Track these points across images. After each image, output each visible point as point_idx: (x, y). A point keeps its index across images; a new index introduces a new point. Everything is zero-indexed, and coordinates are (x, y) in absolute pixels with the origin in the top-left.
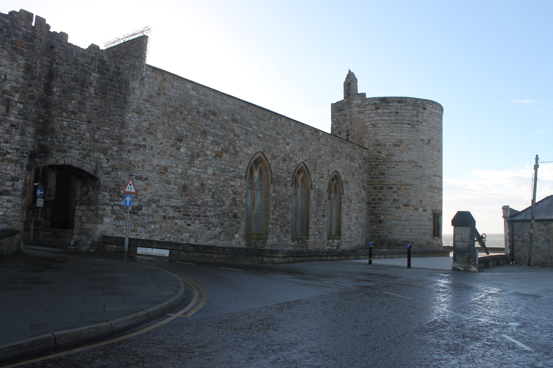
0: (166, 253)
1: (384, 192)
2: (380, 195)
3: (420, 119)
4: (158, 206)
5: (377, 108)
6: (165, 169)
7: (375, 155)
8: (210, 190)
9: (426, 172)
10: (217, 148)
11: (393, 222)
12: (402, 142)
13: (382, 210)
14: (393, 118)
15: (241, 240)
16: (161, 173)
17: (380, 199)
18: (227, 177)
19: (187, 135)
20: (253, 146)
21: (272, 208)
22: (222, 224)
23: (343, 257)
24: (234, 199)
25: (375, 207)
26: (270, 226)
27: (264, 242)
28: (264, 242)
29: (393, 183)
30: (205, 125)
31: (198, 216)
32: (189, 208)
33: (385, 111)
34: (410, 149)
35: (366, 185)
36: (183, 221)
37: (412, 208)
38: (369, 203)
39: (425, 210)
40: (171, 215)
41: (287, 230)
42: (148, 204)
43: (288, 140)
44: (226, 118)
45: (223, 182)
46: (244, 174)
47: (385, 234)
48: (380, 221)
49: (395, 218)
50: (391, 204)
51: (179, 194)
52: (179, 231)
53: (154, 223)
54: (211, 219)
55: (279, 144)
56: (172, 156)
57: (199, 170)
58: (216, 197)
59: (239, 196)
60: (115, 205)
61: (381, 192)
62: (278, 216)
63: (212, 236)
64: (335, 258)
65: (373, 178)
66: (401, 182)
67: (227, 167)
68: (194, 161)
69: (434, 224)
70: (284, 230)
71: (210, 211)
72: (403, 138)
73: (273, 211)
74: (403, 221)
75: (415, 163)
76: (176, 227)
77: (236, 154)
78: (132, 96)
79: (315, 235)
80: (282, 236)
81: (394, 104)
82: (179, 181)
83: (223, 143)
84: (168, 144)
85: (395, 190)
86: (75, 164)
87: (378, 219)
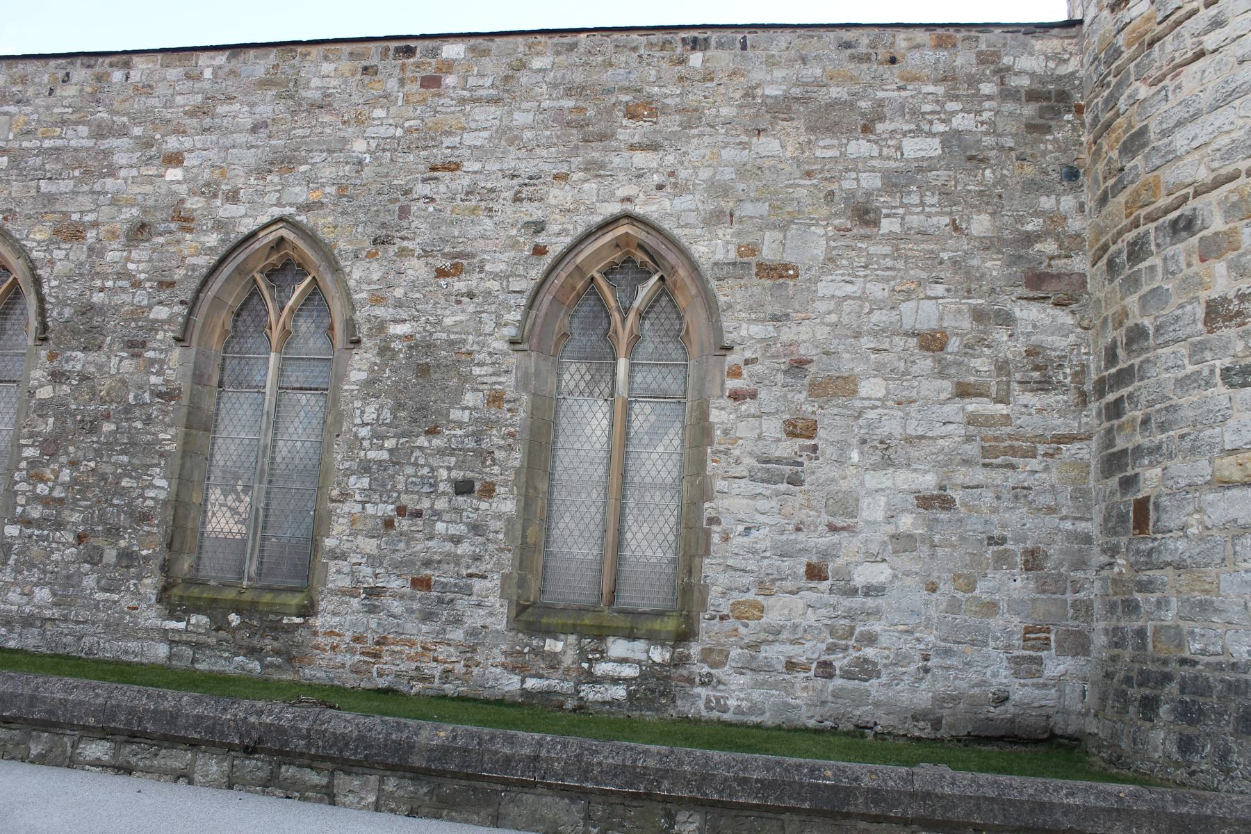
1: (1152, 268)
2: (1132, 301)
13: (1145, 422)
17: (1137, 335)
21: (30, 452)
25: (1115, 410)
26: (12, 530)
29: (1203, 175)
41: (127, 557)
43: (173, 143)
47: (1170, 616)
49: (1229, 468)
50: (1197, 351)
55: (112, 174)
62: (67, 487)
70: (110, 555)
73: (33, 463)
79: (374, 592)
80: (90, 582)
85: (1218, 224)
87: (1130, 498)
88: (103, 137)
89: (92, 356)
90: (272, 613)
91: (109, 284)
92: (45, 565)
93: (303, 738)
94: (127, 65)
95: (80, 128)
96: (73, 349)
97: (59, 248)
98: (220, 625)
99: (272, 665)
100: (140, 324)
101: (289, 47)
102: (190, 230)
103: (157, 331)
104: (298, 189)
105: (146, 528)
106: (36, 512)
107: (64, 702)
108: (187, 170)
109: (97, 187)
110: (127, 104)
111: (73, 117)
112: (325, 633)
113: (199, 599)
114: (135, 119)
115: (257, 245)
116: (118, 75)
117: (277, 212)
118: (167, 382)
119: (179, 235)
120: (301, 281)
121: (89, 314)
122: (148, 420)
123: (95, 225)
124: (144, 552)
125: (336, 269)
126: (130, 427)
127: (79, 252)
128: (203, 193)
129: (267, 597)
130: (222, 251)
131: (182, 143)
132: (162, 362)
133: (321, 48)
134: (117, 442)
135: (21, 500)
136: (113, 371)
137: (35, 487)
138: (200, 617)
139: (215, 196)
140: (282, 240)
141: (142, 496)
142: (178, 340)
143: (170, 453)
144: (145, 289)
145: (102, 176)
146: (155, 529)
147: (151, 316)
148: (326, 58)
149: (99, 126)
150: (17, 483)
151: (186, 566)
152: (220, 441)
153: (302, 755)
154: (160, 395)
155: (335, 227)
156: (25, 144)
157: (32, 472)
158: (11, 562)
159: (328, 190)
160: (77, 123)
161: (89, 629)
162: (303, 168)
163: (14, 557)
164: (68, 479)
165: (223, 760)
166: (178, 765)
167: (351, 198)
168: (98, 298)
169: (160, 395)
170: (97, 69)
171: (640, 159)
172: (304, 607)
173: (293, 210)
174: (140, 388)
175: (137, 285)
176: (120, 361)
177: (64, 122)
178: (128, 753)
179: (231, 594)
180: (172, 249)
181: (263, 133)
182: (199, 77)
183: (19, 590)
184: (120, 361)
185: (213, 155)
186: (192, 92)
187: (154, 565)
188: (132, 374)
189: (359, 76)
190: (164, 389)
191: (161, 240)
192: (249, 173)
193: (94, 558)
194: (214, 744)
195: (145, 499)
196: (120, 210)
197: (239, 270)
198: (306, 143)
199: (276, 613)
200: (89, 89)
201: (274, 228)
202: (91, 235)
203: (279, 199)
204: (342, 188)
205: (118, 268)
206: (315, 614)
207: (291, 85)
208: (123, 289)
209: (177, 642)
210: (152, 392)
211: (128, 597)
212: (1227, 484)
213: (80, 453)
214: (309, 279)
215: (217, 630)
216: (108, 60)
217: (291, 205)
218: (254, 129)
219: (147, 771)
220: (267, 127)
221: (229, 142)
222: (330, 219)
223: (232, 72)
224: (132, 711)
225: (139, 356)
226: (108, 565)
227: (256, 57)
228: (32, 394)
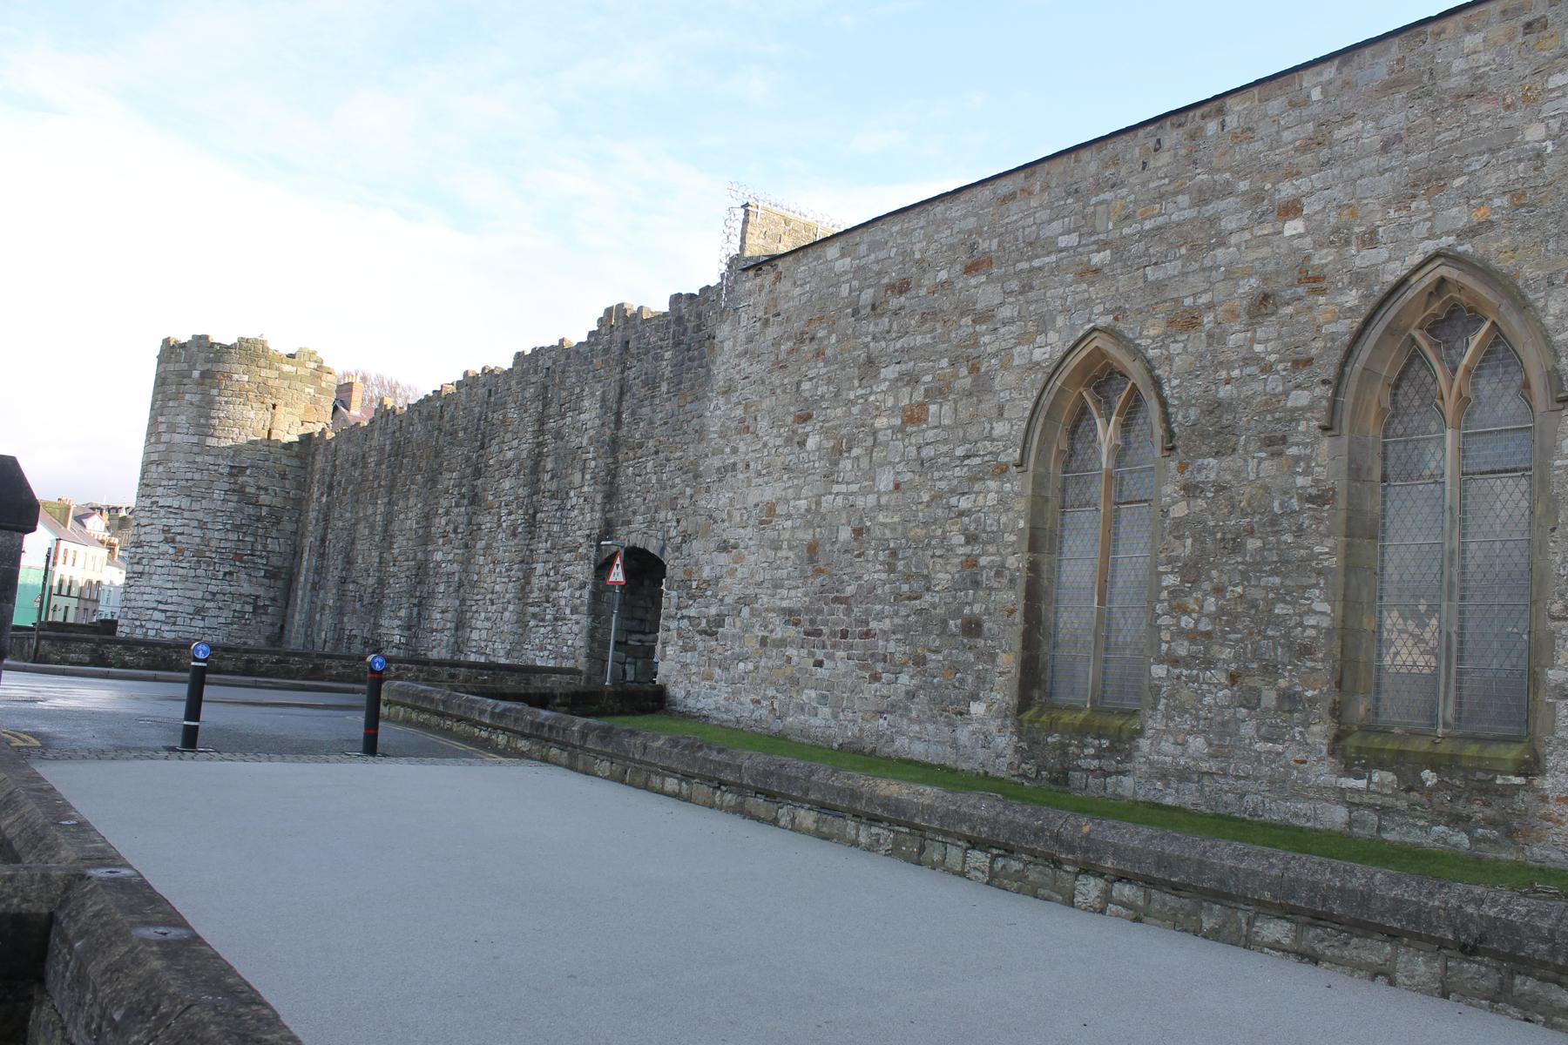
4: (753, 613)
6: (771, 509)
8: (883, 544)
15: (993, 726)
16: (761, 523)
18: (942, 485)
20: (1060, 321)
21: (1170, 580)
22: (920, 661)
23: (554, 751)
24: (971, 562)
26: (1159, 671)
27: (1112, 750)
28: (1112, 750)
31: (844, 634)
32: (820, 612)
36: (804, 652)
40: (778, 634)
41: (1289, 700)
43: (1287, 190)
44: (943, 275)
45: (928, 505)
46: (1017, 455)
51: (797, 574)
52: (794, 681)
53: (745, 659)
54: (881, 643)
58: (900, 565)
59: (991, 549)
60: (683, 617)
63: (884, 705)
64: (523, 745)
67: (943, 449)
68: (837, 464)
70: (1269, 698)
71: (880, 617)
73: (1174, 592)
76: (788, 670)
77: (982, 385)
80: (1248, 729)
82: (800, 534)
83: (926, 372)
86: (640, 545)
88: (1206, 202)
89: (1227, 461)
90: (1480, 769)
91: (1236, 373)
92: (1197, 710)
93: (1544, 940)
94: (1221, 111)
95: (1180, 198)
96: (1204, 456)
97: (1176, 341)
98: (1411, 785)
99: (1485, 839)
100: (1277, 415)
101: (1414, 31)
102: (1323, 292)
103: (1298, 421)
104: (1455, 210)
105: (1309, 664)
106: (1182, 649)
107: (1234, 871)
108: (1308, 218)
109: (1208, 262)
110: (1228, 157)
111: (1171, 188)
112: (1559, 799)
113: (1383, 750)
114: (1239, 174)
115: (1410, 294)
116: (1212, 127)
117: (1430, 246)
118: (1317, 482)
119: (1309, 300)
120: (1476, 329)
121: (1217, 413)
122: (1300, 532)
123: (1211, 306)
124: (1309, 694)
125: (1522, 305)
126: (1278, 542)
127: (1197, 341)
128: (1332, 242)
129: (1472, 750)
130: (1365, 310)
131: (1298, 188)
132: (1308, 459)
133: (1458, 18)
134: (1265, 561)
135: (1165, 636)
136: (1252, 476)
137: (1179, 620)
138: (1384, 774)
139: (1348, 243)
140: (1442, 281)
141: (1301, 624)
142: (1325, 429)
143: (1330, 570)
144: (1277, 372)
145: (1212, 248)
146: (1321, 665)
147: (1289, 404)
148: (1469, 29)
149: (1200, 191)
150: (1159, 616)
151: (1362, 710)
152: (1390, 550)
153: (1543, 964)
154: (1311, 499)
155: (1514, 250)
156: (1126, 231)
157: (1174, 603)
158: (1161, 707)
159: (1497, 202)
160: (1176, 194)
161: (1252, 786)
162: (1458, 182)
163: (1163, 701)
164: (1213, 609)
165: (1435, 960)
166: (1374, 959)
167: (1532, 207)
168: (1225, 392)
169: (1311, 499)
170: (1189, 126)
172: (1525, 762)
173: (1452, 239)
174: (1286, 493)
175: (1268, 369)
176: (1259, 463)
177: (1162, 196)
178: (1313, 938)
179: (1422, 745)
180: (1303, 319)
181: (1397, 150)
182: (1307, 101)
183: (1171, 739)
184: (1259, 463)
185: (1337, 192)
186: (1301, 122)
187: (1322, 709)
188: (1274, 477)
189: (1520, 39)
190: (1314, 491)
191: (1289, 310)
192: (1387, 204)
193: (1251, 701)
194: (1419, 937)
195: (1305, 628)
196: (1237, 285)
197: (1391, 330)
198: (1457, 148)
199: (1487, 771)
200: (1183, 152)
201: (1430, 267)
202: (1208, 319)
203: (1430, 229)
204: (1517, 197)
205: (1243, 352)
206: (1542, 773)
207: (1425, 78)
208: (1252, 377)
209: (1357, 805)
210: (1300, 497)
211: (1294, 747)
213: (1225, 578)
214: (1487, 325)
215: (1409, 790)
216: (1198, 112)
217: (1448, 234)
218: (1386, 147)
219: (1337, 962)
220: (1401, 140)
221: (1355, 172)
222: (1505, 241)
223: (1346, 84)
224: (1314, 887)
225: (1280, 454)
226: (1267, 709)
227: (1374, 57)
228: (1165, 513)
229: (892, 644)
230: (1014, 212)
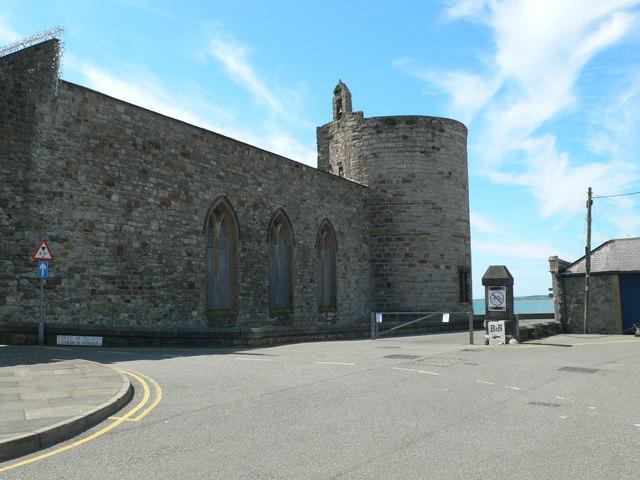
0: (99, 341)
3: (436, 144)
4: (83, 277)
5: (379, 132)
7: (378, 196)
8: (155, 251)
9: (448, 216)
10: (164, 194)
11: (407, 285)
12: (413, 176)
14: (401, 144)
15: (200, 318)
16: (86, 230)
19: (120, 178)
22: (174, 298)
24: (189, 263)
25: (381, 266)
26: (240, 297)
30: (145, 162)
31: (140, 288)
33: (390, 135)
34: (426, 186)
35: (368, 236)
36: (119, 297)
37: (432, 265)
38: (373, 261)
39: (447, 267)
40: (102, 288)
42: (70, 275)
43: (260, 179)
44: (173, 151)
47: (396, 301)
48: (389, 285)
53: (79, 301)
56: (100, 206)
57: (139, 225)
58: (164, 261)
61: (388, 246)
65: (377, 226)
66: (414, 230)
69: (461, 285)
71: (156, 281)
72: (415, 171)
74: (420, 282)
75: (434, 204)
77: (189, 201)
78: (40, 125)
81: (402, 125)
82: (111, 241)
84: (93, 190)
171: (327, 205)
212: (407, 282)
229: (162, 293)
230: (198, 143)
